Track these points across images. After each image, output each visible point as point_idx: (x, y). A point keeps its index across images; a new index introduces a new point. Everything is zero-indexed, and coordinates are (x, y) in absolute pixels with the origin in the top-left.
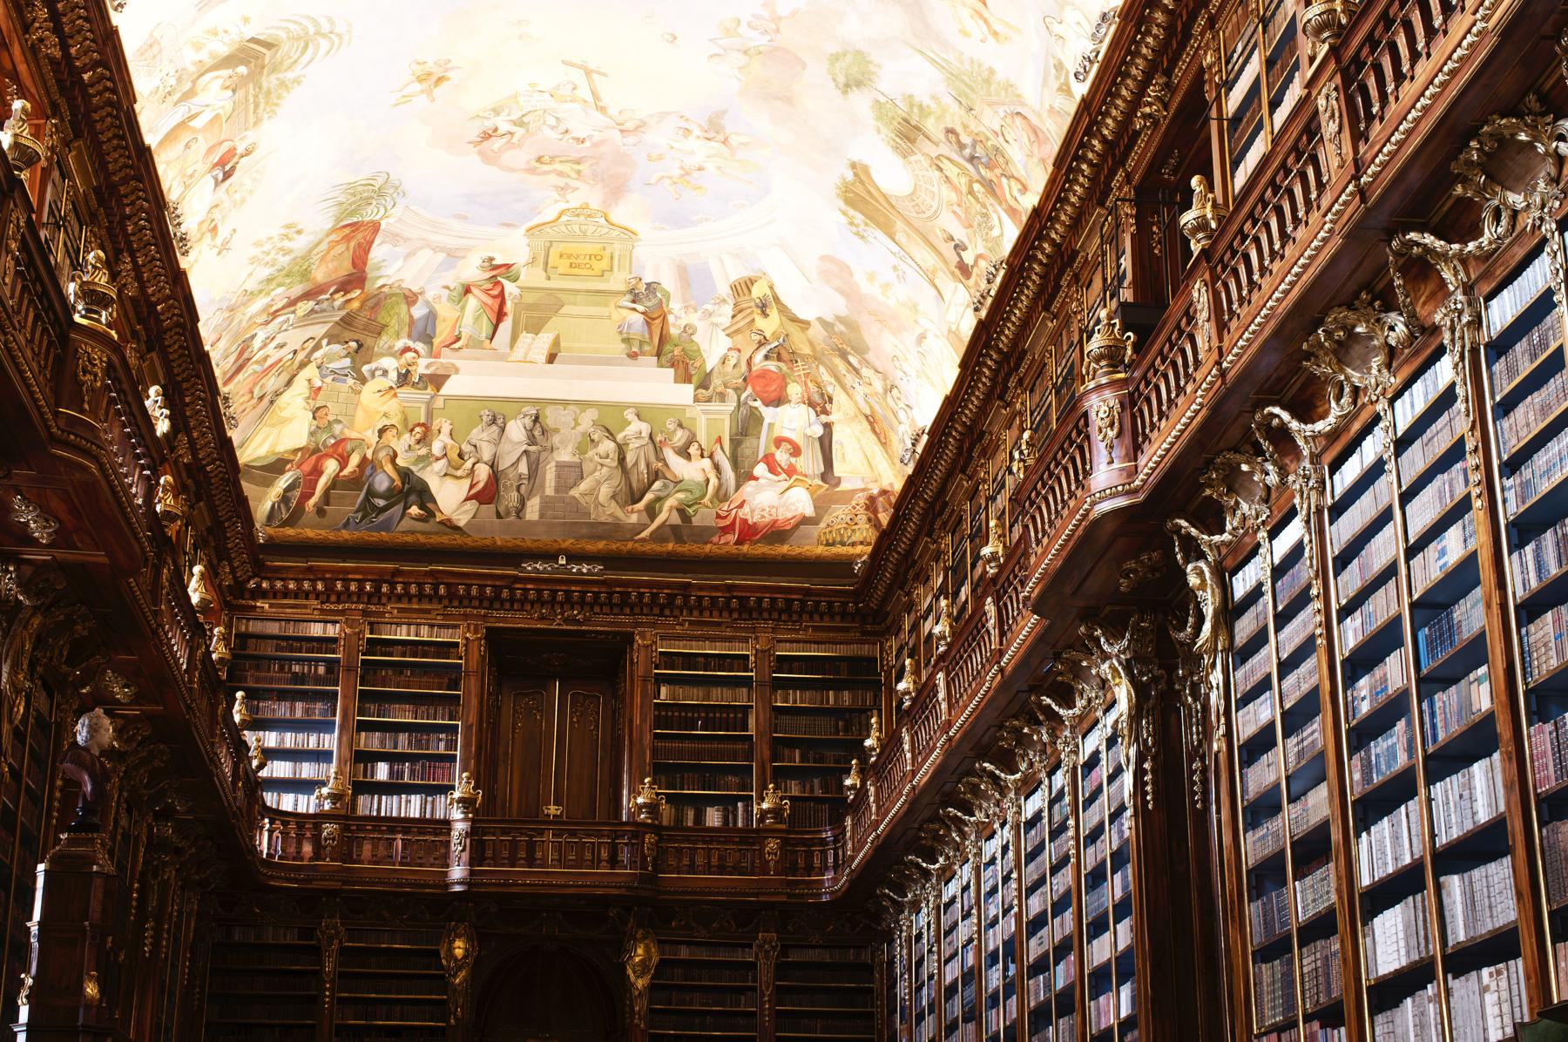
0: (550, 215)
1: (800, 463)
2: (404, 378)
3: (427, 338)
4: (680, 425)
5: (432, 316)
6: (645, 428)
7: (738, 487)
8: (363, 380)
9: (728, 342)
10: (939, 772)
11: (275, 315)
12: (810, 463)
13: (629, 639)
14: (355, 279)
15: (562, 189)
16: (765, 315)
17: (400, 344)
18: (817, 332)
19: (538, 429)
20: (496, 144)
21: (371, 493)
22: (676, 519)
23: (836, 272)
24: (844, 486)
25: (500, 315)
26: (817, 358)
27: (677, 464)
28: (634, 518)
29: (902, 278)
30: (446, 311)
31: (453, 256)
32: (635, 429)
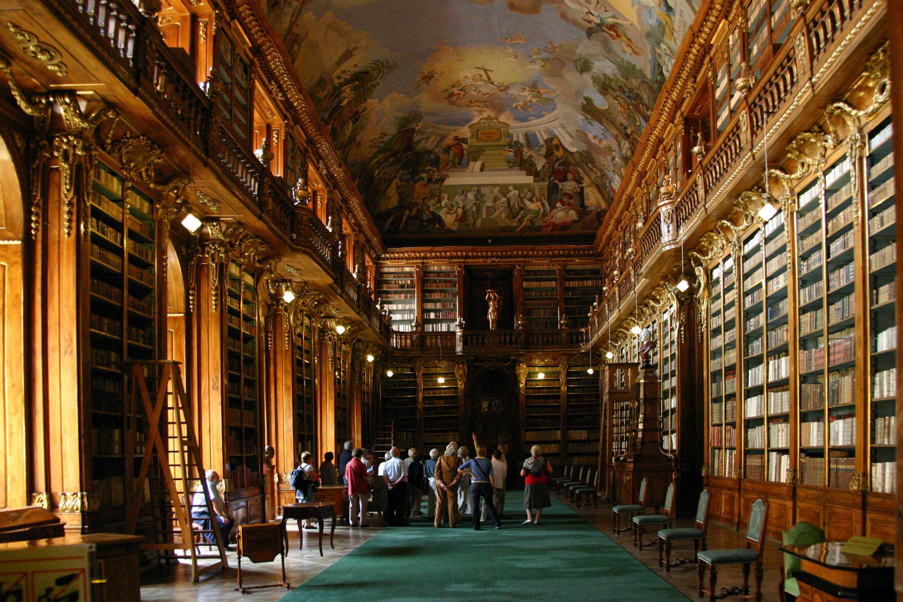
0: (476, 120)
1: (572, 201)
2: (430, 181)
3: (437, 166)
4: (529, 191)
5: (438, 158)
6: (517, 192)
7: (551, 210)
8: (416, 182)
9: (545, 161)
11: (382, 163)
12: (575, 201)
13: (514, 266)
14: (409, 147)
15: (480, 112)
16: (558, 150)
17: (427, 168)
18: (577, 156)
19: (479, 196)
20: (454, 98)
21: (422, 221)
22: (529, 224)
23: (582, 135)
24: (589, 209)
26: (577, 165)
27: (527, 202)
28: (514, 224)
29: (606, 138)
30: (441, 155)
31: (443, 138)
32: (514, 193)
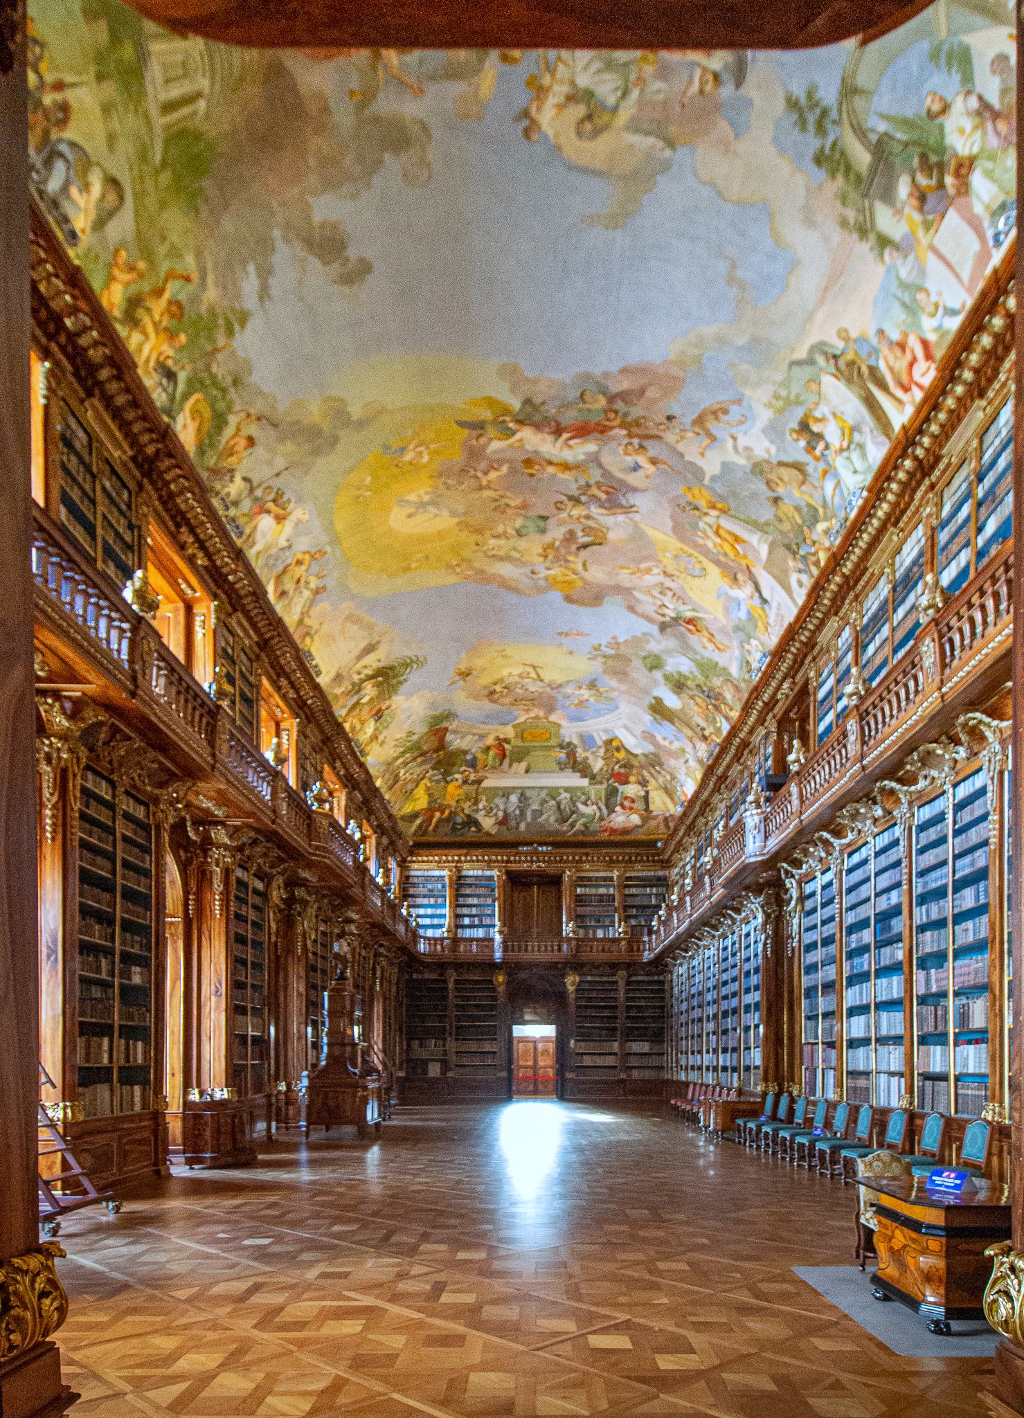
10: (688, 929)
15: (527, 711)
25: (504, 756)
